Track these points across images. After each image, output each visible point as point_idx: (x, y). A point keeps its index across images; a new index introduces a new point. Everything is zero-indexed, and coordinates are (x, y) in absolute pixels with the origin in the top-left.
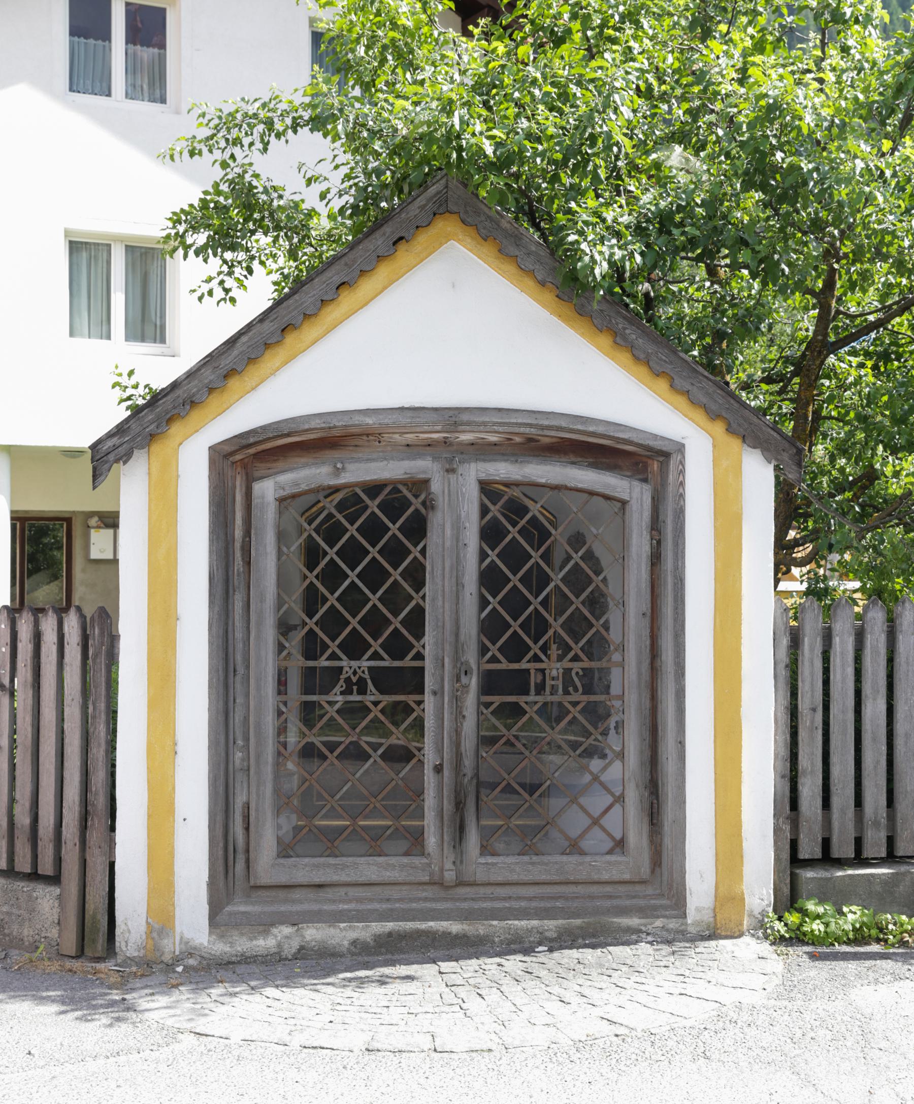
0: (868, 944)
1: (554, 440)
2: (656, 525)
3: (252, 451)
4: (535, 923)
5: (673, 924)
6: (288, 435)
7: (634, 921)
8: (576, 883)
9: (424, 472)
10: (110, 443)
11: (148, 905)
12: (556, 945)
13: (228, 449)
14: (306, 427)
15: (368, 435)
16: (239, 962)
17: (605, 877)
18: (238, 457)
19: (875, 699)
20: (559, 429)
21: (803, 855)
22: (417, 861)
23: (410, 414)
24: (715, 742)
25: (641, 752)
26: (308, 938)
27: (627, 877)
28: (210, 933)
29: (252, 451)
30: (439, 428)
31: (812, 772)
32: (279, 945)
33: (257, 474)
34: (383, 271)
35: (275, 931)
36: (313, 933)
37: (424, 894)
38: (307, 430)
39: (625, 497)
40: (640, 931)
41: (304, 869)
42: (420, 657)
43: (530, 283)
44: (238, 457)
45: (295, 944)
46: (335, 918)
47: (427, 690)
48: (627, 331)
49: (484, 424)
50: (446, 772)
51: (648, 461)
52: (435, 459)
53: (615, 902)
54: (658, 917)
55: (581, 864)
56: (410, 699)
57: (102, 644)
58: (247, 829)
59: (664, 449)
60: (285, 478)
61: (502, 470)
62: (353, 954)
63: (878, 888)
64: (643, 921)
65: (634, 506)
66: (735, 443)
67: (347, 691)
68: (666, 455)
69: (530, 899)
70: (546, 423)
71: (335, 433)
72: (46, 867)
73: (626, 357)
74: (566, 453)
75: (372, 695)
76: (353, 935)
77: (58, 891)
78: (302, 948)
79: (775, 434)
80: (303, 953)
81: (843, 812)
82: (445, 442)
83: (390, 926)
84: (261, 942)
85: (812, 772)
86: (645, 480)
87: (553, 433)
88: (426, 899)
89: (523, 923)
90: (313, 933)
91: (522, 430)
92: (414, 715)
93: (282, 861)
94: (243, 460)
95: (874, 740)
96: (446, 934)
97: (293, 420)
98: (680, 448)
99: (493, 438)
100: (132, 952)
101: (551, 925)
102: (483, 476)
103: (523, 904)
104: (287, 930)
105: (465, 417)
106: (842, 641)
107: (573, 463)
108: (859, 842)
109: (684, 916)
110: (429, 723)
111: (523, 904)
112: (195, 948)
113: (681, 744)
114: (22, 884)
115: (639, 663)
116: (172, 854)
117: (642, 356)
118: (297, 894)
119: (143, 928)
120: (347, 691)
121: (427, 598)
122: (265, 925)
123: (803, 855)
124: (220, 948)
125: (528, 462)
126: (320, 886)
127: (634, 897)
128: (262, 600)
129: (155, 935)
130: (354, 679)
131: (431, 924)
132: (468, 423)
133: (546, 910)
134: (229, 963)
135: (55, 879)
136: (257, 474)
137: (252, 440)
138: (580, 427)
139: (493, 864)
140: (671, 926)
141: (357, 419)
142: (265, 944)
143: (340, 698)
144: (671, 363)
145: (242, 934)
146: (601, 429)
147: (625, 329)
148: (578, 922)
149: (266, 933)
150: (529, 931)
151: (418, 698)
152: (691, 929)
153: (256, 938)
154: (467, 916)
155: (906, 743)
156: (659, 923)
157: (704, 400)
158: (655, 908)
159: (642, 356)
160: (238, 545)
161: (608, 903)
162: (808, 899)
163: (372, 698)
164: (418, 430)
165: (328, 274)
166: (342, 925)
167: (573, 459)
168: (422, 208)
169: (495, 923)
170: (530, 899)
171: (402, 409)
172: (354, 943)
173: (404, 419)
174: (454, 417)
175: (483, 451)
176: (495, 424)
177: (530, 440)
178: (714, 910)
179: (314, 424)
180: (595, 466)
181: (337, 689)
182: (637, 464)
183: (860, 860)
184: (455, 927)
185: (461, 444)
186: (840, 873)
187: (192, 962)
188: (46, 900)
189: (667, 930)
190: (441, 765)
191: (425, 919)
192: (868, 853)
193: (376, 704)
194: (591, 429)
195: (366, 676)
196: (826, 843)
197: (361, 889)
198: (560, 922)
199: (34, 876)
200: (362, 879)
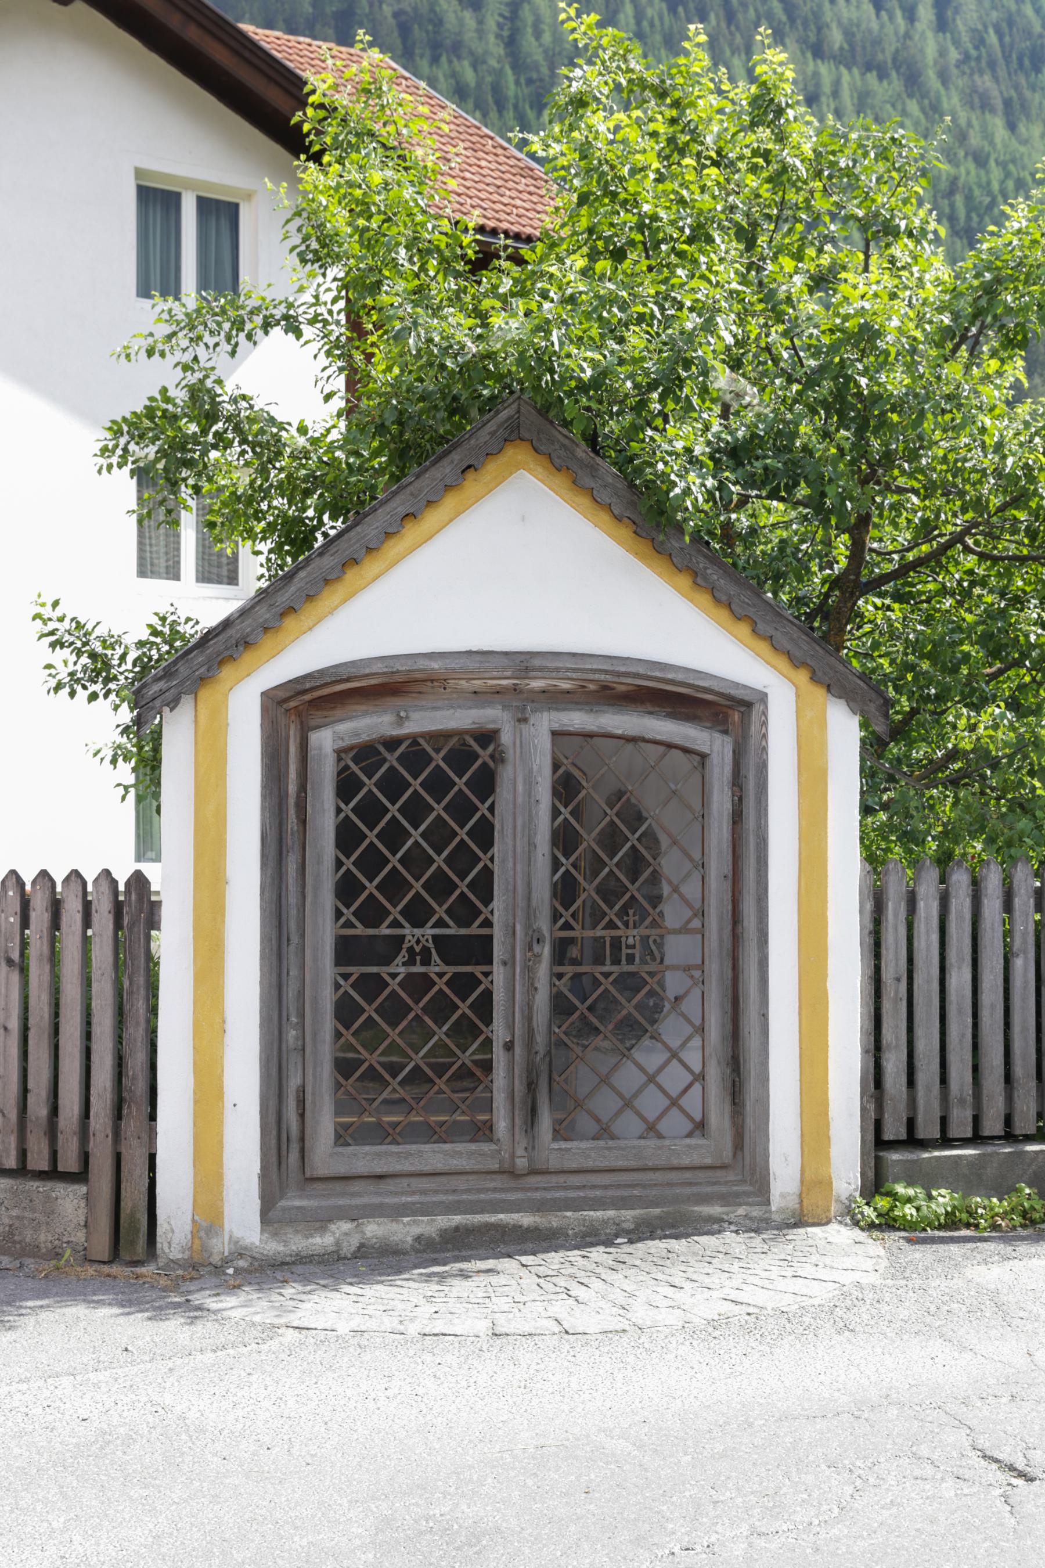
0: (958, 1229)
1: (630, 688)
2: (737, 780)
3: (307, 697)
4: (611, 1213)
5: (756, 1212)
6: (347, 680)
7: (716, 1210)
8: (654, 1169)
9: (494, 722)
10: (156, 688)
11: (195, 1201)
12: (634, 1237)
13: (282, 695)
14: (367, 671)
15: (432, 681)
16: (294, 1263)
17: (686, 1161)
18: (292, 704)
19: (959, 968)
20: (636, 676)
21: (888, 1135)
22: (486, 1147)
23: (478, 658)
24: (800, 1014)
25: (723, 1026)
26: (369, 1234)
27: (708, 1161)
28: (262, 1231)
29: (307, 697)
30: (508, 674)
31: (897, 1046)
32: (338, 1243)
33: (313, 723)
34: (450, 502)
35: (332, 1227)
36: (374, 1229)
37: (492, 1185)
38: (367, 675)
39: (705, 749)
40: (722, 1220)
41: (364, 1158)
42: (488, 923)
43: (605, 517)
44: (292, 704)
45: (355, 1242)
46: (397, 1212)
47: (495, 960)
48: (709, 571)
49: (557, 670)
50: (518, 1050)
51: (731, 711)
52: (505, 707)
53: (695, 1189)
54: (740, 1205)
55: (660, 1148)
56: (477, 970)
57: (141, 911)
58: (302, 1116)
59: (746, 698)
60: (343, 727)
61: (577, 720)
62: (417, 1251)
63: (966, 1171)
64: (725, 1209)
65: (715, 760)
66: (820, 693)
67: (411, 962)
68: (749, 705)
69: (605, 1187)
70: (623, 669)
72: (69, 1162)
73: (705, 599)
74: (642, 702)
75: (437, 967)
76: (417, 1230)
77: (84, 1189)
78: (362, 1246)
79: (862, 684)
80: (363, 1252)
81: (928, 1089)
82: (515, 689)
83: (457, 1219)
84: (317, 1240)
85: (897, 1046)
86: (725, 732)
87: (629, 681)
88: (495, 1190)
89: (599, 1214)
90: (374, 1229)
91: (597, 677)
92: (482, 987)
93: (340, 1149)
94: (298, 707)
95: (960, 1011)
96: (517, 1227)
97: (352, 663)
98: (763, 697)
99: (565, 685)
100: (175, 1254)
101: (628, 1216)
102: (556, 727)
103: (599, 1193)
104: (346, 1226)
105: (537, 662)
106: (926, 905)
107: (651, 713)
108: (944, 1121)
109: (768, 1203)
110: (499, 997)
111: (599, 1193)
112: (246, 1248)
113: (765, 1016)
114: (36, 1184)
115: (721, 930)
116: (221, 1144)
117: (724, 598)
118: (356, 1186)
119: (188, 1228)
120: (411, 962)
121: (496, 859)
122: (321, 1222)
123: (888, 1135)
124: (273, 1247)
125: (604, 712)
126: (381, 1177)
127: (714, 1184)
128: (319, 861)
129: (202, 1234)
130: (418, 949)
131: (501, 1216)
132: (541, 669)
133: (623, 1199)
134: (283, 1264)
135: (81, 1176)
136: (313, 723)
137: (308, 686)
138: (658, 674)
139: (567, 1150)
140: (754, 1214)
141: (422, 664)
142: (321, 1242)
143: (402, 969)
144: (754, 606)
145: (297, 1232)
146: (680, 677)
147: (706, 568)
148: (656, 1211)
149: (323, 1229)
150: (605, 1222)
151: (486, 968)
152: (776, 1217)
153: (312, 1236)
154: (540, 1207)
155: (992, 1015)
156: (741, 1211)
157: (788, 646)
158: (737, 1195)
159: (724, 598)
160: (292, 801)
161: (688, 1191)
162: (894, 1182)
163: (437, 969)
164: (487, 675)
165: (392, 504)
166: (406, 1219)
167: (651, 709)
168: (493, 434)
169: (569, 1214)
170: (605, 1187)
171: (469, 653)
172: (418, 1239)
173: (471, 664)
174: (524, 662)
175: (554, 699)
176: (568, 670)
177: (605, 688)
178: (800, 1195)
179: (377, 668)
180: (673, 716)
181: (399, 960)
182: (717, 714)
183: (946, 1141)
184: (526, 1220)
185: (532, 691)
186: (926, 1155)
187: (242, 1263)
188: (69, 1201)
189: (751, 1219)
190: (512, 1042)
191: (496, 1212)
192: (954, 1132)
193: (441, 975)
194: (670, 676)
195: (431, 945)
196: (911, 1123)
197: (424, 1180)
198: (638, 1212)
199: (53, 1174)
200: (427, 1169)
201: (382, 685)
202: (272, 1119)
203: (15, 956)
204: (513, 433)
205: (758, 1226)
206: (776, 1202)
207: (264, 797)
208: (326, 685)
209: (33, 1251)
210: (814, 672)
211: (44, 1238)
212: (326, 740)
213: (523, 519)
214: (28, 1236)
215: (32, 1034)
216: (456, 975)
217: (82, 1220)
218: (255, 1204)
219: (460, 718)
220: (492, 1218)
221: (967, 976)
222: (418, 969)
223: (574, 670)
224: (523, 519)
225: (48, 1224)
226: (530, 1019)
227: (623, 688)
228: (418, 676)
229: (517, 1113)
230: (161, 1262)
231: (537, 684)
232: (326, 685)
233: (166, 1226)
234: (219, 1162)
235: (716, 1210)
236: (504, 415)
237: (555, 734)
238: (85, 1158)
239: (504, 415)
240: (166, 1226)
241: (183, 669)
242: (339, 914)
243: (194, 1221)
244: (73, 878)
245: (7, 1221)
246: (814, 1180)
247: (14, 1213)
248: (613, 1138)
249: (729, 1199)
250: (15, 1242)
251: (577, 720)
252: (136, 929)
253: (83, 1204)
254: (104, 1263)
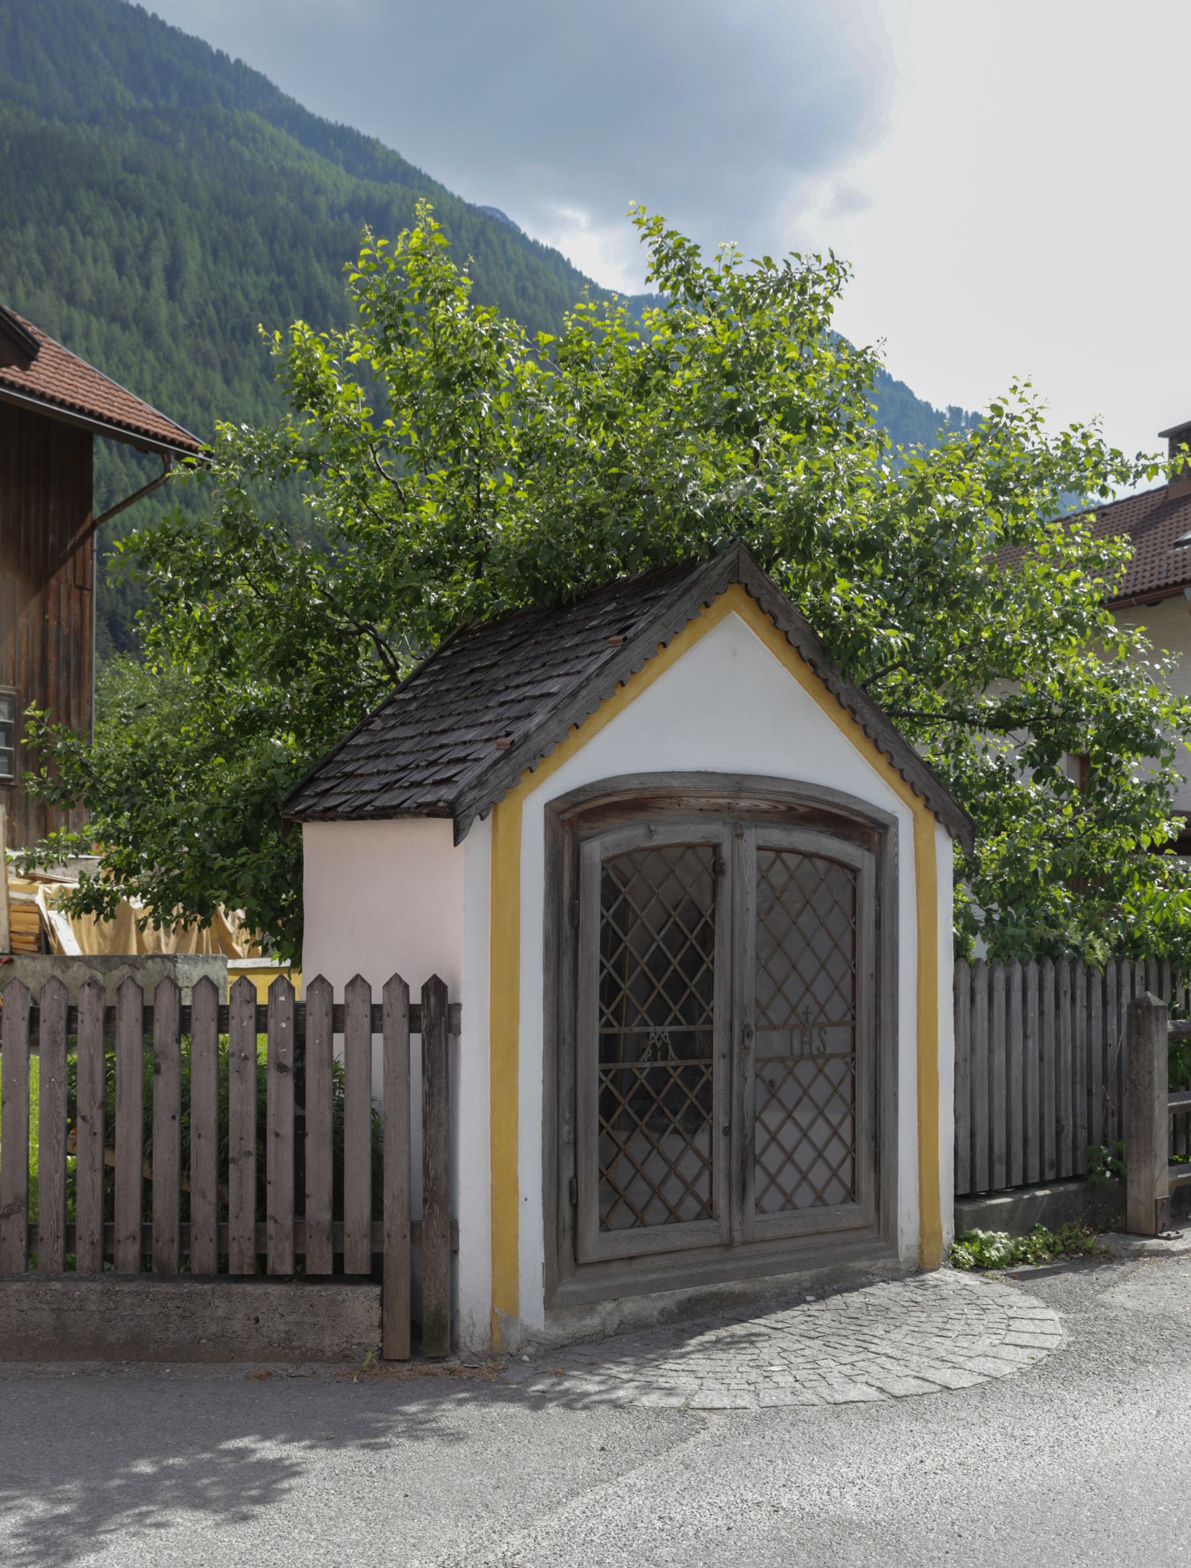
3: (579, 809)
4: (796, 1274)
5: (890, 1264)
6: (609, 795)
7: (863, 1264)
10: (471, 796)
11: (494, 1293)
13: (562, 806)
14: (626, 787)
17: (845, 1225)
18: (568, 815)
20: (814, 799)
22: (711, 1224)
24: (919, 1092)
26: (626, 1312)
27: (860, 1223)
28: (546, 1317)
32: (603, 1323)
33: (583, 833)
34: (686, 635)
35: (599, 1308)
36: (631, 1307)
39: (858, 864)
40: (868, 1273)
41: (624, 1242)
42: (710, 1021)
43: (792, 658)
44: (568, 815)
45: (616, 1320)
46: (648, 1289)
47: (716, 1053)
50: (735, 1134)
52: (725, 824)
56: (700, 1063)
57: (442, 1014)
58: (575, 1207)
60: (609, 839)
62: (661, 1324)
66: (930, 818)
67: (654, 1058)
70: (805, 793)
71: (647, 794)
72: (358, 1262)
73: (858, 734)
75: (673, 1061)
76: (661, 1304)
77: (377, 1290)
78: (621, 1323)
80: (622, 1329)
82: (729, 807)
83: (690, 1291)
84: (588, 1322)
86: (869, 850)
90: (631, 1307)
91: (786, 799)
92: (704, 1079)
93: (605, 1235)
94: (574, 817)
97: (615, 778)
99: (764, 806)
100: (476, 1348)
101: (807, 1275)
102: (761, 843)
104: (609, 1306)
105: (748, 784)
109: (896, 1255)
110: (719, 1087)
112: (534, 1335)
113: (896, 1095)
114: (310, 1288)
116: (517, 1236)
117: (873, 734)
118: (614, 1268)
119: (487, 1320)
120: (654, 1058)
121: (716, 962)
122: (589, 1304)
124: (556, 1332)
126: (632, 1258)
129: (502, 1325)
130: (658, 1045)
131: (721, 1285)
132: (748, 790)
134: (563, 1346)
135: (375, 1275)
136: (583, 833)
137: (581, 799)
138: (828, 798)
142: (592, 1322)
143: (648, 1065)
146: (843, 801)
149: (592, 1311)
151: (707, 1061)
152: (903, 1266)
153: (583, 1318)
154: (748, 1274)
156: (880, 1264)
160: (566, 907)
162: (971, 1228)
163: (673, 1064)
165: (650, 633)
168: (721, 575)
171: (698, 773)
174: (738, 783)
175: (759, 817)
177: (791, 809)
178: (921, 1247)
179: (634, 784)
181: (645, 1056)
183: (992, 1194)
184: (737, 1286)
187: (530, 1350)
188: (360, 1304)
190: (730, 1127)
191: (716, 1281)
193: (675, 1068)
194: (836, 800)
195: (668, 1041)
198: (814, 1271)
199: (339, 1275)
200: (669, 1247)
201: (634, 801)
202: (553, 1211)
203: (289, 1061)
204: (734, 576)
205: (895, 1276)
206: (903, 1254)
207: (547, 903)
208: (595, 798)
209: (316, 1356)
210: (927, 799)
211: (329, 1341)
212: (595, 851)
213: (735, 653)
214: (310, 1341)
215: (309, 1141)
216: (686, 1067)
217: (376, 1320)
218: (540, 1292)
219: (694, 833)
220: (713, 1288)
221: (1004, 1056)
222: (660, 1064)
223: (771, 792)
224: (735, 653)
225: (333, 1327)
226: (742, 1105)
227: (802, 809)
228: (661, 793)
229: (734, 1191)
230: (464, 1355)
231: (744, 804)
232: (595, 798)
233: (468, 1320)
234: (515, 1254)
235: (863, 1264)
236: (729, 559)
237: (759, 848)
238: (377, 1260)
239: (729, 559)
240: (468, 1320)
241: (493, 779)
242: (602, 1014)
243: (493, 1313)
244: (359, 982)
245: (282, 1327)
246: (928, 1232)
247: (291, 1319)
248: (795, 1208)
249: (872, 1255)
250: (293, 1348)
251: (776, 836)
252: (436, 1033)
253: (376, 1304)
254: (404, 1361)
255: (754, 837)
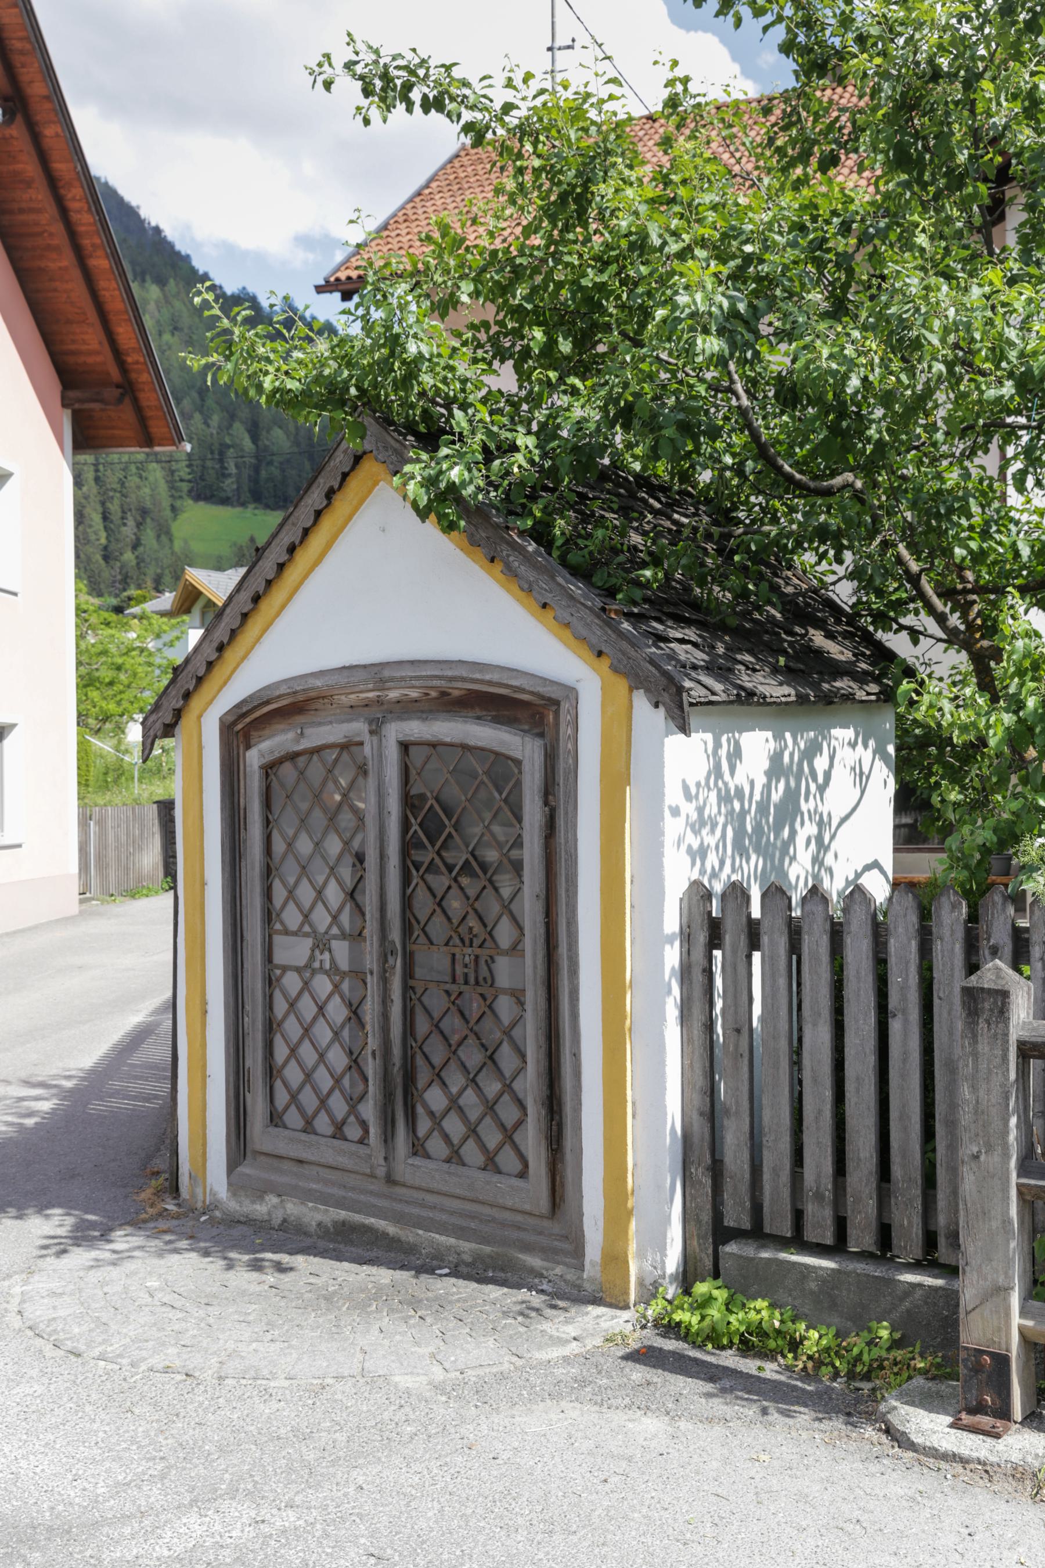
1: (463, 692)
2: (549, 790)
3: (248, 720)
4: (452, 1241)
7: (535, 1261)
8: (483, 1203)
9: (358, 735)
12: (464, 1269)
14: (277, 693)
15: (324, 697)
16: (245, 1223)
17: (509, 1203)
18: (239, 727)
19: (815, 1025)
21: (729, 1222)
23: (346, 673)
25: (538, 1061)
26: (289, 1212)
27: (527, 1207)
29: (248, 720)
30: (371, 686)
31: (737, 1113)
32: (269, 1213)
36: (293, 1208)
37: (372, 1187)
38: (279, 697)
39: (517, 754)
40: (541, 1276)
46: (307, 1195)
48: (511, 559)
49: (402, 679)
51: (533, 709)
53: (523, 1235)
54: (558, 1263)
55: (488, 1183)
59: (553, 696)
60: (265, 745)
61: (415, 729)
63: (813, 1285)
64: (546, 1264)
65: (526, 767)
68: (557, 703)
69: (452, 1213)
71: (300, 698)
74: (472, 707)
76: (319, 1217)
78: (285, 1221)
79: (653, 669)
81: (775, 1171)
83: (343, 1214)
84: (258, 1207)
85: (737, 1113)
87: (459, 685)
88: (371, 1193)
89: (442, 1239)
95: (815, 1080)
96: (385, 1235)
98: (571, 693)
99: (414, 694)
101: (467, 1247)
102: (401, 738)
103: (444, 1217)
105: (387, 673)
106: (771, 940)
107: (479, 718)
108: (798, 1215)
109: (582, 1268)
111: (444, 1217)
113: (576, 1056)
115: (535, 954)
123: (729, 1222)
124: (233, 1205)
125: (436, 719)
126: (301, 1162)
127: (541, 1233)
128: (253, 869)
131: (372, 1220)
132: (392, 679)
133: (462, 1229)
134: (239, 1222)
137: (244, 709)
138: (478, 676)
139: (419, 1167)
140: (568, 1277)
141: (318, 683)
144: (551, 592)
145: (247, 1196)
146: (495, 677)
147: (508, 556)
148: (487, 1249)
150: (449, 1248)
152: (587, 1285)
154: (399, 1218)
155: (858, 1090)
156: (559, 1270)
157: (584, 632)
158: (556, 1251)
159: (526, 586)
161: (515, 1235)
164: (357, 689)
166: (310, 1204)
167: (479, 713)
169: (421, 1232)
170: (452, 1213)
172: (335, 1223)
173: (342, 679)
174: (378, 673)
175: (406, 709)
176: (411, 678)
177: (444, 694)
180: (498, 720)
182: (533, 716)
183: (798, 1241)
185: (389, 702)
186: (765, 1255)
189: (565, 1281)
192: (811, 1235)
194: (488, 677)
196: (757, 1209)
197: (327, 1171)
220: (371, 1221)
228: (313, 694)
231: (393, 695)
235: (535, 1261)
251: (415, 729)
255: (395, 731)
